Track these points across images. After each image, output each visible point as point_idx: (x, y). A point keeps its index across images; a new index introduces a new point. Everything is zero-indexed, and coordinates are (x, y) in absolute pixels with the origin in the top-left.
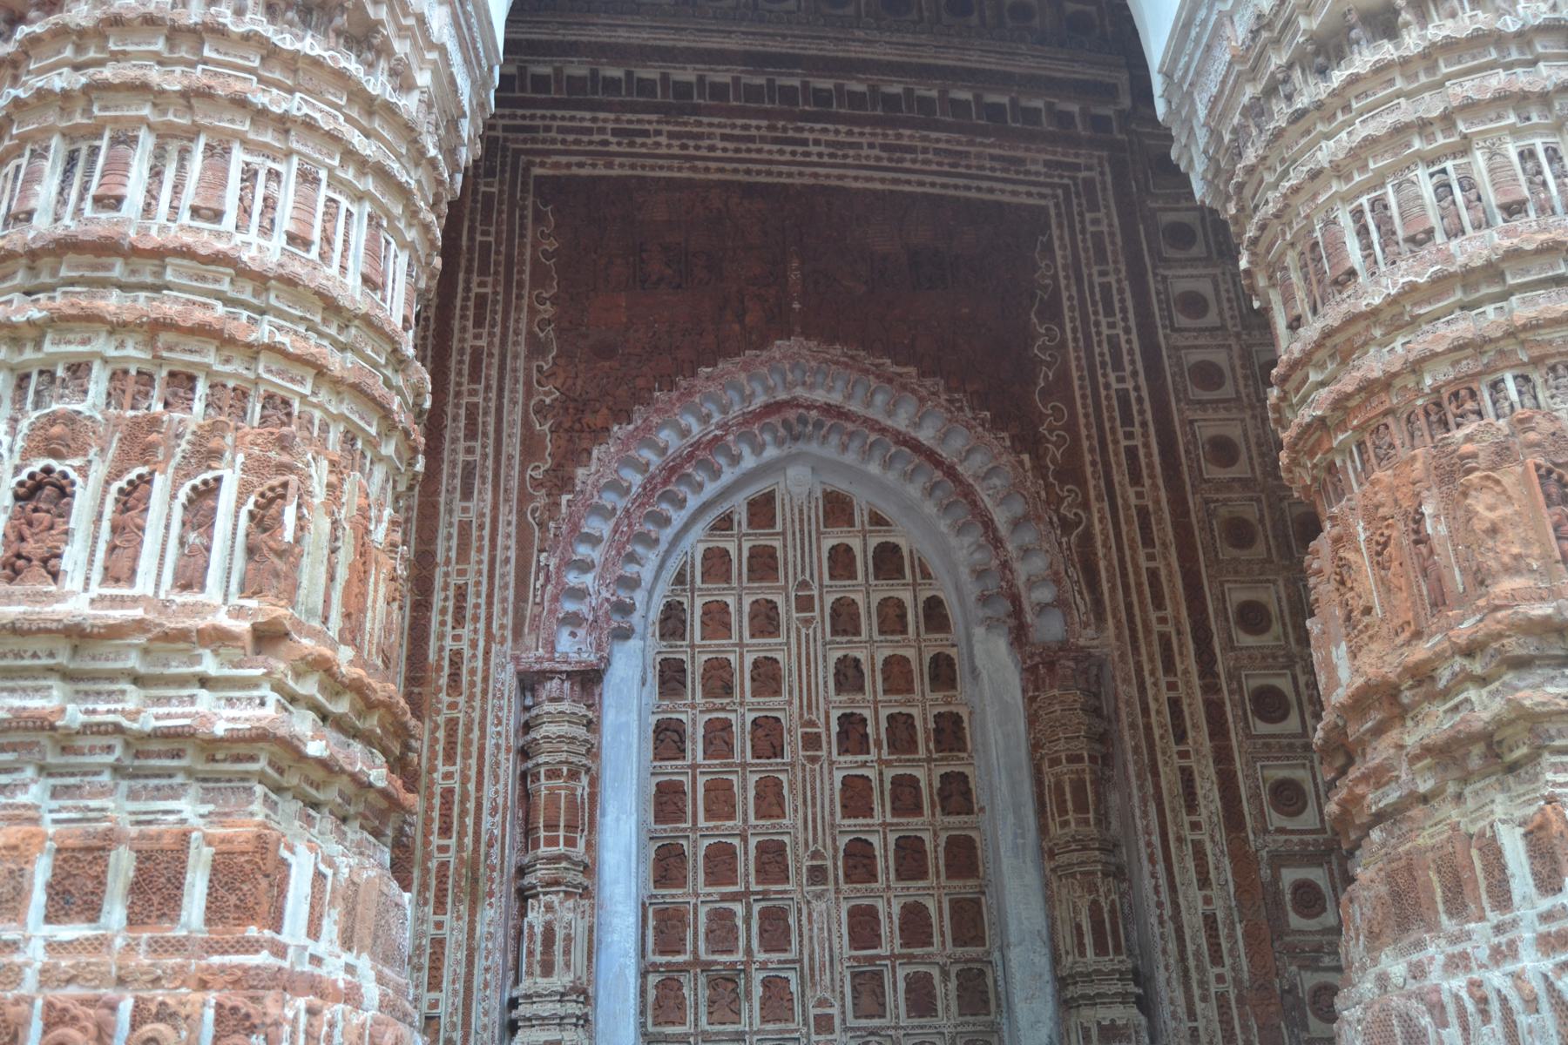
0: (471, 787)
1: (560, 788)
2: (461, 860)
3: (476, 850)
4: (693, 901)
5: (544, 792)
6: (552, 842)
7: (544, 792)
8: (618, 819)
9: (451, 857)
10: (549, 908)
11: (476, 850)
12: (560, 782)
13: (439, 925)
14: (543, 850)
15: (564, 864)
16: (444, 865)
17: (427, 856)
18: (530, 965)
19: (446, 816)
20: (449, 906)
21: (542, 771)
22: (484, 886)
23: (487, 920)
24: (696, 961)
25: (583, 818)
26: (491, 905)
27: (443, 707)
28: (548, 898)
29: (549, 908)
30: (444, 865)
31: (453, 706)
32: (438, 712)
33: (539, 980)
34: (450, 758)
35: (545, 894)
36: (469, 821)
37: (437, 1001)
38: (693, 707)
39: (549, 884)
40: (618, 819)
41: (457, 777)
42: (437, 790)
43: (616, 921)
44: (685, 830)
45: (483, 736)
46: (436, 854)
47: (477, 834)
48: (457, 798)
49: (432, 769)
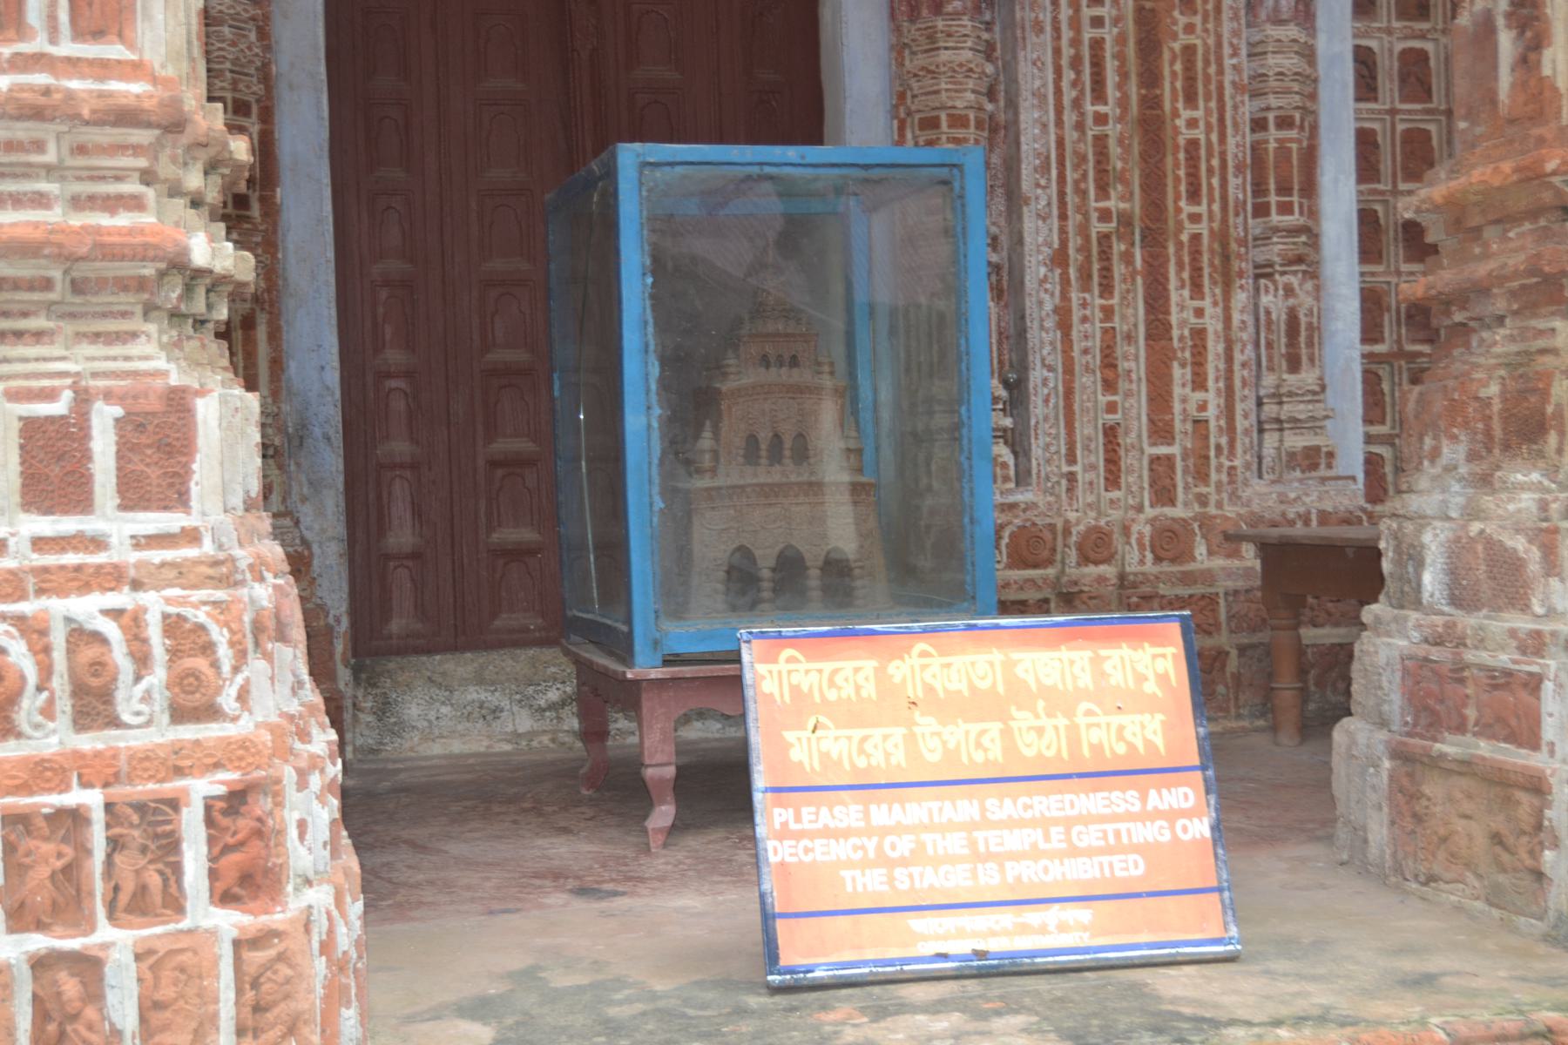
0: (1214, 137)
1: (1291, 140)
2: (1211, 231)
3: (1224, 220)
4: (1394, 280)
5: (1272, 145)
6: (1285, 209)
7: (1272, 145)
8: (1336, 181)
9: (1203, 228)
10: (1289, 291)
11: (1224, 220)
12: (1293, 133)
13: (1199, 312)
14: (1275, 218)
15: (1303, 238)
16: (1196, 238)
17: (1180, 227)
18: (1270, 359)
19: (1193, 176)
20: (1206, 290)
21: (1271, 116)
22: (1236, 265)
23: (1240, 305)
24: (1401, 354)
25: (1304, 180)
26: (1241, 287)
27: (1179, 28)
28: (1285, 278)
29: (1289, 291)
30: (1196, 238)
31: (1189, 29)
32: (1175, 37)
33: (1285, 376)
34: (1191, 100)
35: (1283, 273)
36: (1215, 182)
37: (1205, 402)
38: (1389, 31)
39: (1291, 263)
40: (1336, 181)
41: (1202, 124)
42: (1181, 141)
43: (1339, 306)
44: (1382, 193)
45: (1220, 72)
46: (1187, 224)
47: (1224, 198)
48: (1203, 152)
49: (1175, 114)
